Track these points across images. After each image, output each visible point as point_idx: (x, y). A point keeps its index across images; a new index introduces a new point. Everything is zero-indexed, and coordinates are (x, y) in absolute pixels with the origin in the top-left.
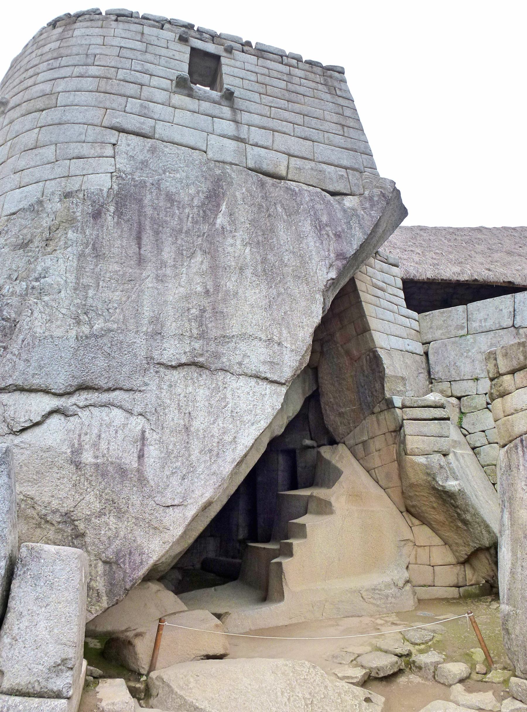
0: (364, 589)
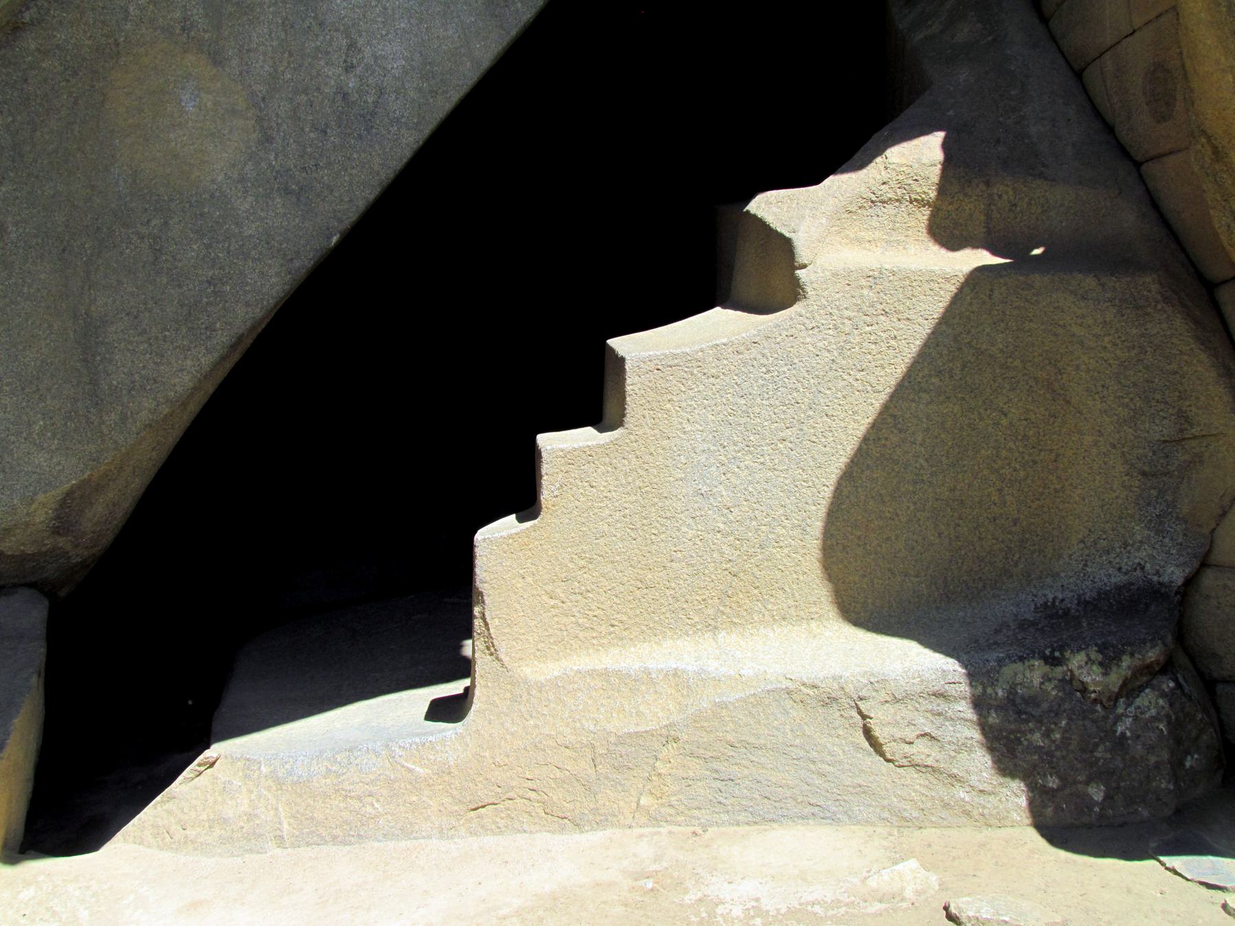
0: (883, 696)
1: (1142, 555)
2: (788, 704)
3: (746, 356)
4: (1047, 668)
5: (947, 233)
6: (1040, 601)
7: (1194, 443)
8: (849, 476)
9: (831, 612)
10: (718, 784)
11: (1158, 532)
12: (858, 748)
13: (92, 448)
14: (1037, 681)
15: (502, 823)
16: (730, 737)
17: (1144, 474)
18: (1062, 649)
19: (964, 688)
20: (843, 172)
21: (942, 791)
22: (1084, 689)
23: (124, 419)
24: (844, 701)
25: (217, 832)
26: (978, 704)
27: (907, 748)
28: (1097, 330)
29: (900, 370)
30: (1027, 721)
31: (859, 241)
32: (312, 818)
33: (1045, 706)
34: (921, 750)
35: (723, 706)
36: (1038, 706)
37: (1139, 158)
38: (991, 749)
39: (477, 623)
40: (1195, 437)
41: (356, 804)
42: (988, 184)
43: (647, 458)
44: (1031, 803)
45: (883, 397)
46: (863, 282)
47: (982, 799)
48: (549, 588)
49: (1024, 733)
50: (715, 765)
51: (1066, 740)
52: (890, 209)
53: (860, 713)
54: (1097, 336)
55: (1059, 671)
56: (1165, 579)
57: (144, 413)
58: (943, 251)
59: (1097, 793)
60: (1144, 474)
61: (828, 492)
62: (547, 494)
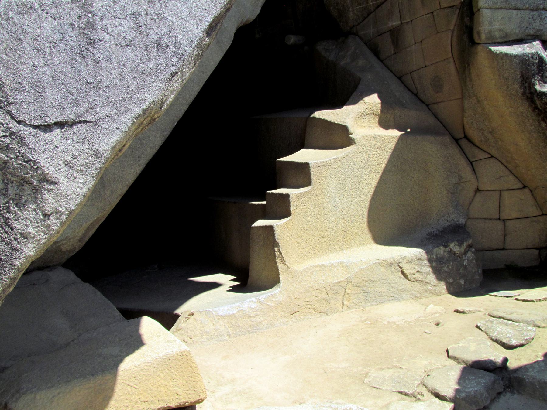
0: (406, 261)
1: (453, 216)
2: (380, 267)
3: (342, 162)
4: (444, 248)
5: (385, 124)
6: (427, 233)
7: (462, 184)
8: (373, 198)
9: (372, 242)
10: (365, 294)
11: (457, 210)
12: (400, 278)
13: (102, 204)
14: (442, 253)
15: (302, 317)
16: (366, 279)
17: (451, 193)
18: (446, 242)
19: (425, 256)
20: (349, 105)
21: (424, 287)
22: (455, 254)
23: (112, 192)
24: (395, 264)
25: (205, 337)
26: (430, 260)
27: (414, 276)
28: (436, 152)
29: (384, 166)
30: (442, 264)
31: (362, 126)
32: (239, 326)
33: (445, 259)
34: (417, 276)
35: (362, 270)
36: (444, 259)
37: (428, 103)
38: (435, 273)
39: (277, 253)
40: (463, 182)
41: (253, 319)
42: (394, 109)
43: (319, 195)
44: (447, 287)
45: (380, 174)
46: (371, 139)
47: (434, 288)
48: (296, 240)
49: (442, 267)
50: (364, 288)
51: (452, 268)
52: (368, 117)
53: (400, 267)
54: (436, 154)
55: (447, 249)
56: (460, 223)
57: (119, 190)
58: (384, 130)
59: (462, 282)
60: (451, 193)
61: (368, 204)
62: (293, 209)
